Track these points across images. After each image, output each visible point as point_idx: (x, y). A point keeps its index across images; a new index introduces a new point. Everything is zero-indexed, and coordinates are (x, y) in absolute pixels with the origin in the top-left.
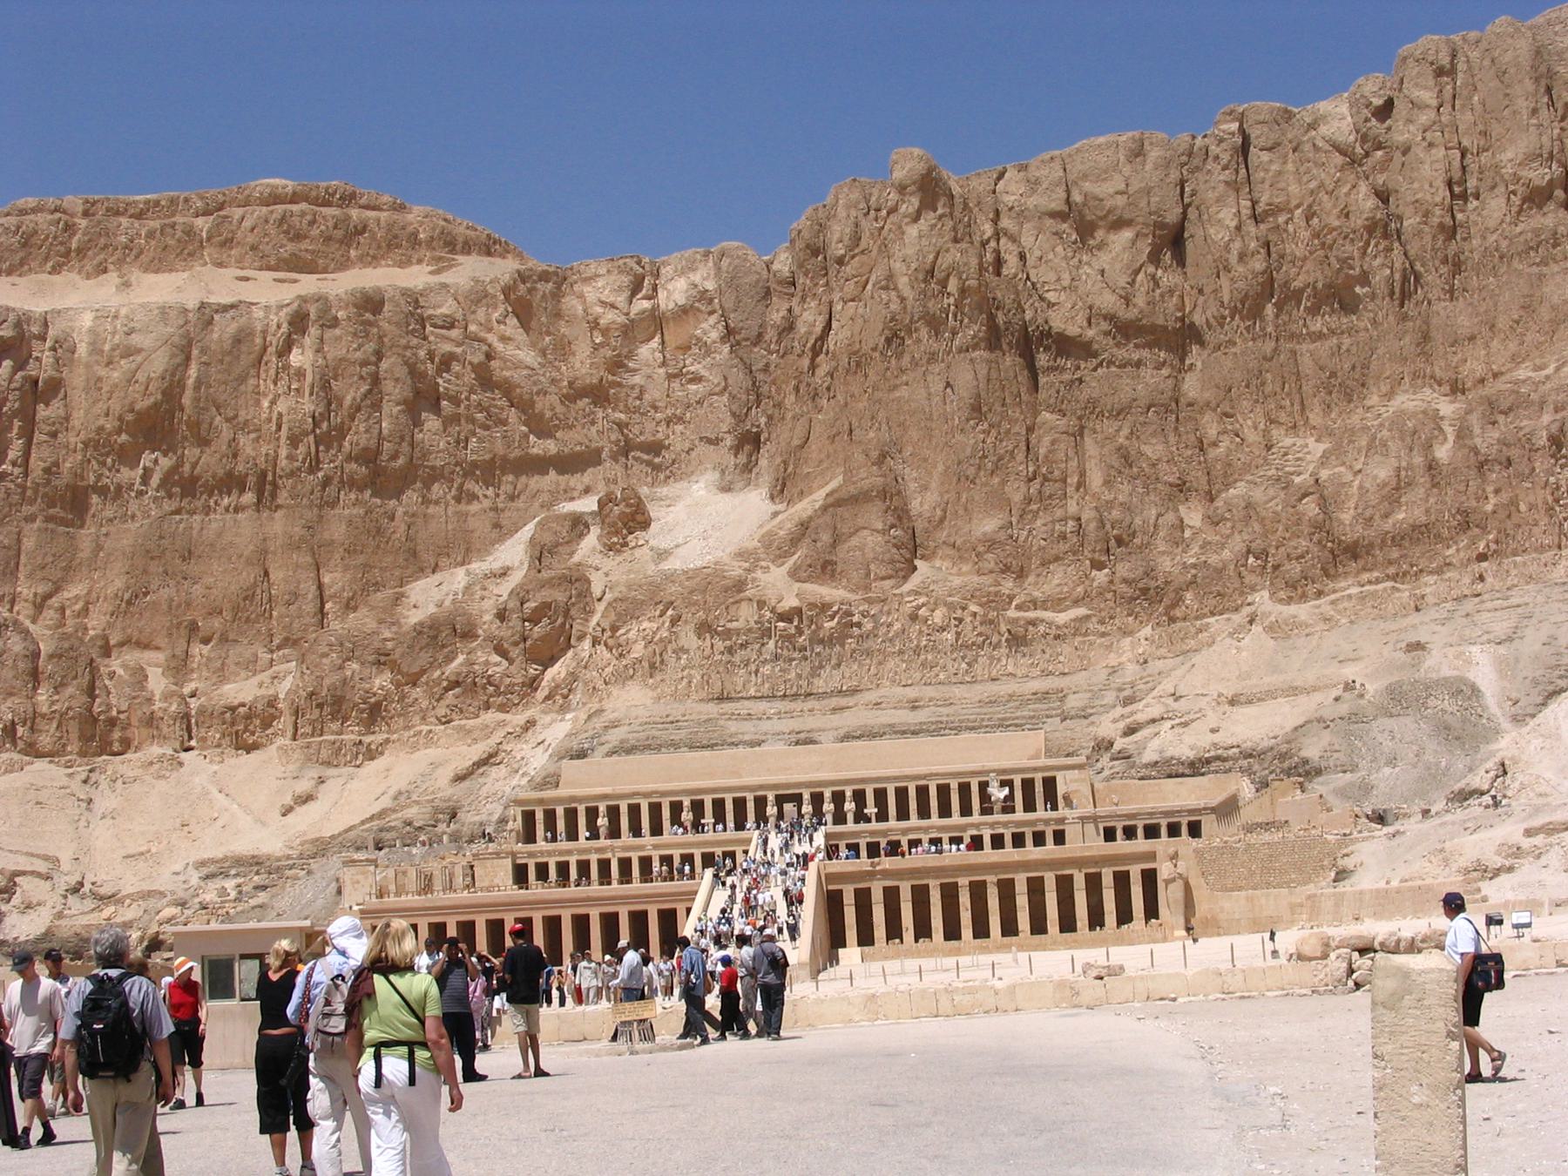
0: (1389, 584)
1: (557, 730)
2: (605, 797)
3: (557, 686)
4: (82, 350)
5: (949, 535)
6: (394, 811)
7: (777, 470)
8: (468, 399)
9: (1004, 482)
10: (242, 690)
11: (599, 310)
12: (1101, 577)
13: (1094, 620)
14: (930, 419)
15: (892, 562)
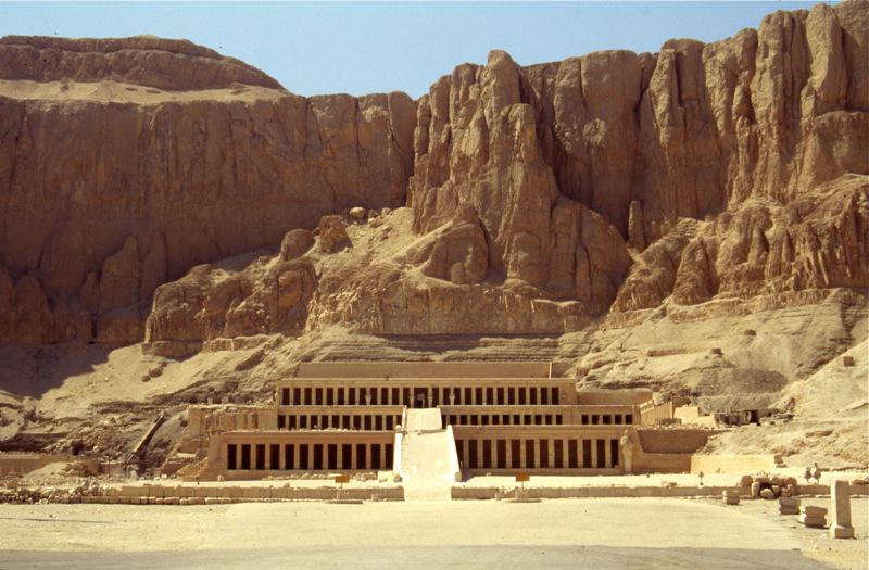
0: (736, 299)
1: (293, 345)
6: (205, 382)
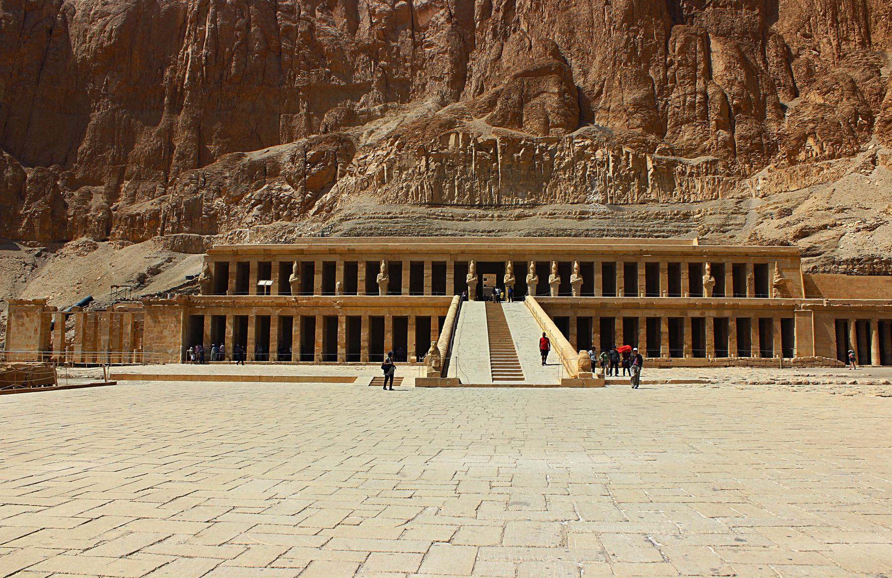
2: (301, 252)
3: (323, 206)
4: (79, 13)
5: (605, 103)
7: (478, 80)
8: (297, 52)
9: (647, 68)
10: (144, 207)
11: (376, 4)
12: (723, 134)
13: (720, 163)
14: (592, 26)
15: (563, 115)
